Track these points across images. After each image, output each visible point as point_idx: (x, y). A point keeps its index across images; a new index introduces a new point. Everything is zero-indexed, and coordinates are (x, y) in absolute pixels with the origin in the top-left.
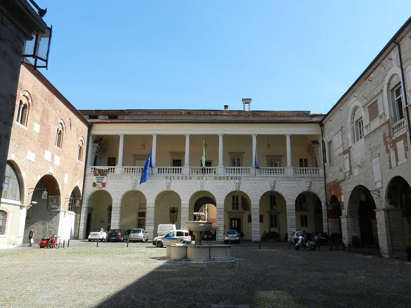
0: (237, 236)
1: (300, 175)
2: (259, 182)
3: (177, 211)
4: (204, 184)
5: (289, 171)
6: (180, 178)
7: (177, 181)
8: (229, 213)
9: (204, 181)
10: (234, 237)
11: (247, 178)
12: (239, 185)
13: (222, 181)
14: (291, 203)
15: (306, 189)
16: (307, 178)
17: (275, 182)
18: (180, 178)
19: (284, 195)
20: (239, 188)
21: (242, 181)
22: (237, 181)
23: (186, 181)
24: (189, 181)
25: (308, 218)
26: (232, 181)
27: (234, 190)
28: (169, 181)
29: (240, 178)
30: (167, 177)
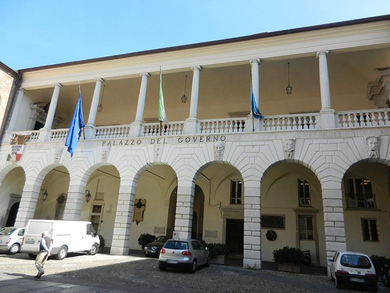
0: (185, 254)
1: (351, 126)
2: (263, 143)
3: (145, 205)
4: (159, 152)
5: (326, 119)
6: (124, 142)
7: (120, 147)
8: (224, 209)
9: (160, 146)
10: (178, 255)
11: (237, 137)
12: (221, 151)
13: (192, 145)
14: (331, 187)
15: (367, 155)
16: (369, 131)
17: (294, 141)
18: (124, 142)
19: (313, 167)
20: (221, 155)
21: (228, 145)
22: (218, 143)
23: (133, 147)
24: (136, 147)
25: (378, 223)
26: (208, 143)
27: (212, 160)
28: (106, 147)
29: (223, 138)
30: (104, 142)
